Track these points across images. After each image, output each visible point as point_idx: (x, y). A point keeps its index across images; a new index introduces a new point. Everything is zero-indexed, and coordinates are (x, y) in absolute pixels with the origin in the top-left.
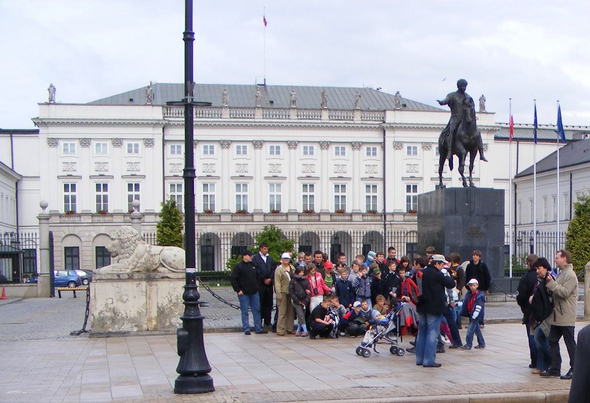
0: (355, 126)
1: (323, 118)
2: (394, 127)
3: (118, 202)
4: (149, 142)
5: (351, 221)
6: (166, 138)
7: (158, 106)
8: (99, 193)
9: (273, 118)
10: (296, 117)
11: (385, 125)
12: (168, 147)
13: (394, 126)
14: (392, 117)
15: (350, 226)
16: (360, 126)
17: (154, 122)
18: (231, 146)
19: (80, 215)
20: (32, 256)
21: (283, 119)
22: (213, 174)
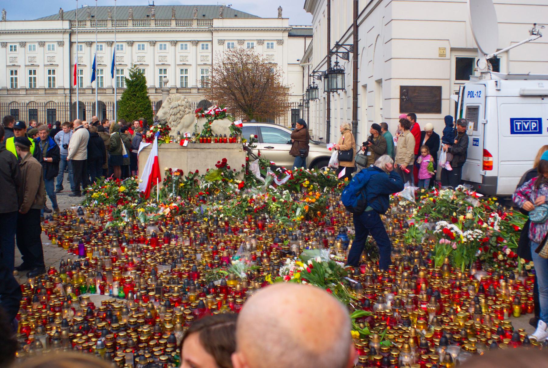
0: (192, 30)
1: (172, 25)
2: (218, 30)
3: (42, 82)
4: (61, 44)
5: (190, 93)
6: (72, 41)
7: (66, 20)
8: (50, 76)
9: (139, 26)
10: (155, 26)
11: (211, 29)
12: (75, 46)
13: (217, 29)
14: (217, 23)
15: (190, 96)
16: (195, 30)
17: (63, 31)
18: (156, 45)
19: (19, 90)
20: (35, 113)
21: (146, 26)
22: (102, 63)
